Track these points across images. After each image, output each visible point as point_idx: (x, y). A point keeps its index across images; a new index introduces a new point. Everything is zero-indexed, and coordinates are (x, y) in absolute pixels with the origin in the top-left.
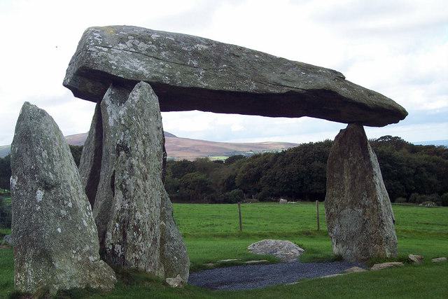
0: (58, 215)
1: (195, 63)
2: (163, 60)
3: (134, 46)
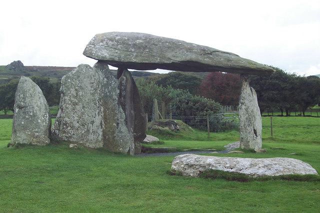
0: (24, 118)
1: (133, 50)
2: (119, 49)
3: (107, 44)
